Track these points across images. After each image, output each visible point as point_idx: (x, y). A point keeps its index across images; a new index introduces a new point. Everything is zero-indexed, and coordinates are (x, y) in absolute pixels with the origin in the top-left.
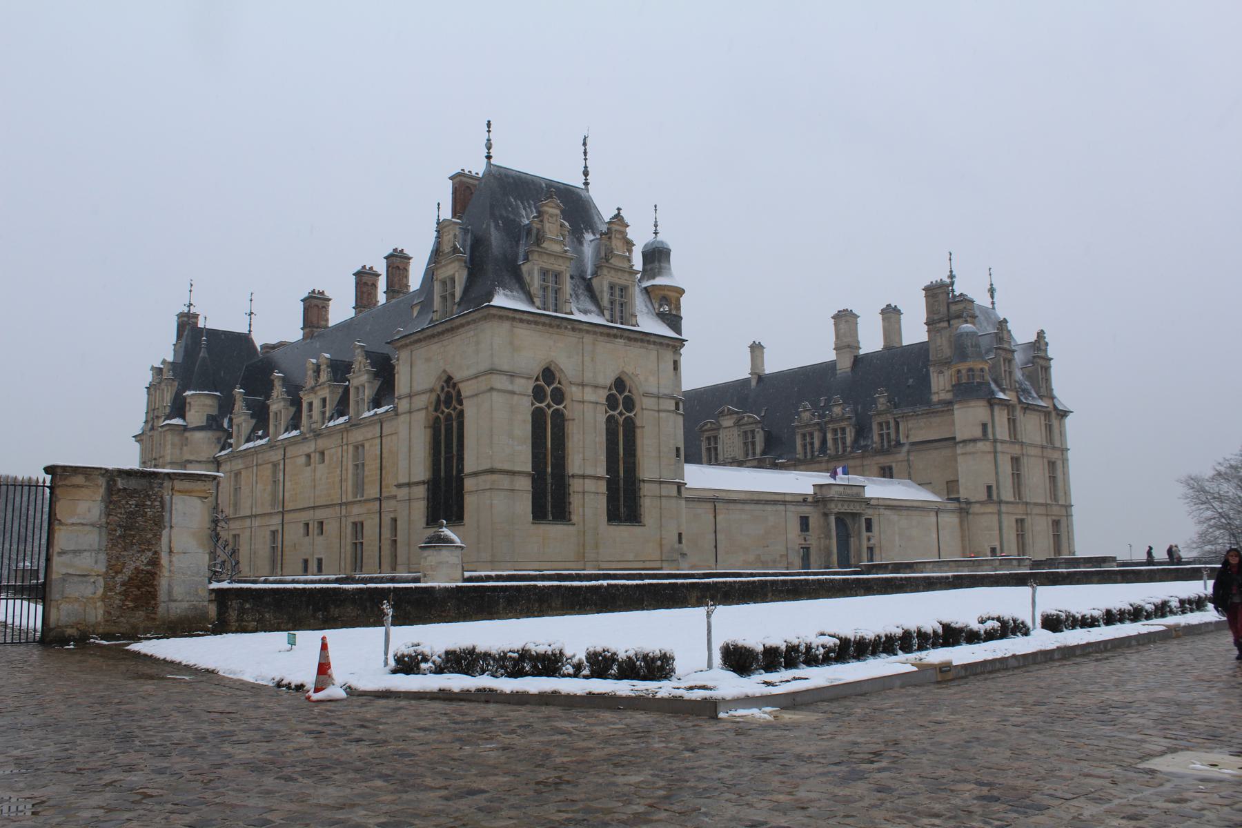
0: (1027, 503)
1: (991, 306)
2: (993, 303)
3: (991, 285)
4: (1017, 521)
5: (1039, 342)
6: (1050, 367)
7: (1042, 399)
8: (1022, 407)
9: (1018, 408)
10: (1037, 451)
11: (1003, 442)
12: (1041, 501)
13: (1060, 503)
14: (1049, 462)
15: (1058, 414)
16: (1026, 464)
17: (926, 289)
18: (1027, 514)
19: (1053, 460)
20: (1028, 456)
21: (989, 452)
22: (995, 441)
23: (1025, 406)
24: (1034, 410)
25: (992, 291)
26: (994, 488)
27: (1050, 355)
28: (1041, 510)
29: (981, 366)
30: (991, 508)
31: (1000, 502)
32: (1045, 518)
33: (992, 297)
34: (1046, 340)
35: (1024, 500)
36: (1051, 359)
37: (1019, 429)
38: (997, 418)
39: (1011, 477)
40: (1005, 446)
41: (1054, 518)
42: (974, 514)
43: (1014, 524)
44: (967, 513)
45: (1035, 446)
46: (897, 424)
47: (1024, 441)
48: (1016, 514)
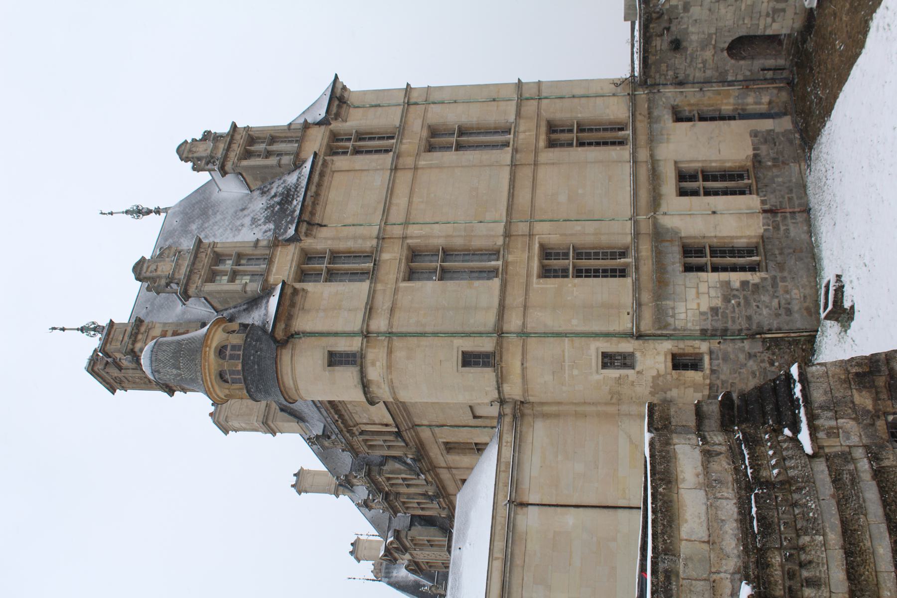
0: (507, 235)
1: (163, 215)
2: (158, 211)
3: (127, 212)
4: (546, 273)
5: (199, 159)
6: (247, 129)
7: (304, 161)
8: (307, 235)
9: (308, 243)
10: (404, 178)
11: (370, 310)
12: (505, 174)
13: (512, 118)
14: (431, 148)
15: (337, 116)
16: (426, 230)
17: (113, 391)
18: (531, 235)
19: (425, 133)
20: (406, 223)
21: (390, 352)
22: (366, 334)
23: (304, 227)
24: (317, 194)
25: (139, 212)
26: (469, 345)
27: (225, 129)
28: (525, 174)
29: (212, 356)
30: (513, 362)
31: (500, 333)
32: (542, 172)
33: (149, 212)
34: (199, 137)
35: (500, 242)
36: (234, 126)
37: (350, 245)
38: (319, 327)
39: (450, 285)
40: (379, 298)
41: (542, 143)
42: (525, 391)
43: (552, 284)
44: (522, 402)
45: (391, 191)
46: (362, 433)
47: (375, 231)
48: (529, 275)
